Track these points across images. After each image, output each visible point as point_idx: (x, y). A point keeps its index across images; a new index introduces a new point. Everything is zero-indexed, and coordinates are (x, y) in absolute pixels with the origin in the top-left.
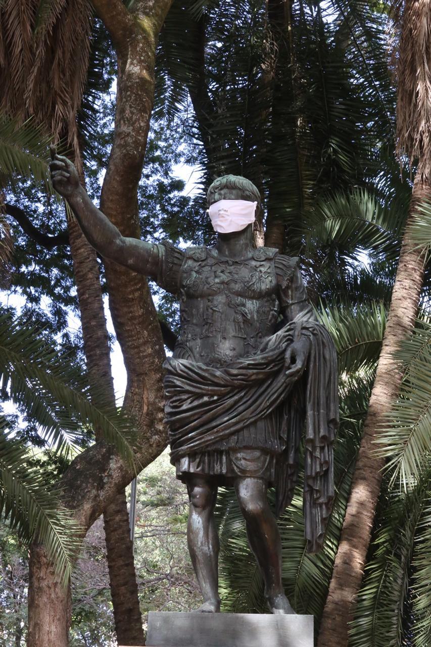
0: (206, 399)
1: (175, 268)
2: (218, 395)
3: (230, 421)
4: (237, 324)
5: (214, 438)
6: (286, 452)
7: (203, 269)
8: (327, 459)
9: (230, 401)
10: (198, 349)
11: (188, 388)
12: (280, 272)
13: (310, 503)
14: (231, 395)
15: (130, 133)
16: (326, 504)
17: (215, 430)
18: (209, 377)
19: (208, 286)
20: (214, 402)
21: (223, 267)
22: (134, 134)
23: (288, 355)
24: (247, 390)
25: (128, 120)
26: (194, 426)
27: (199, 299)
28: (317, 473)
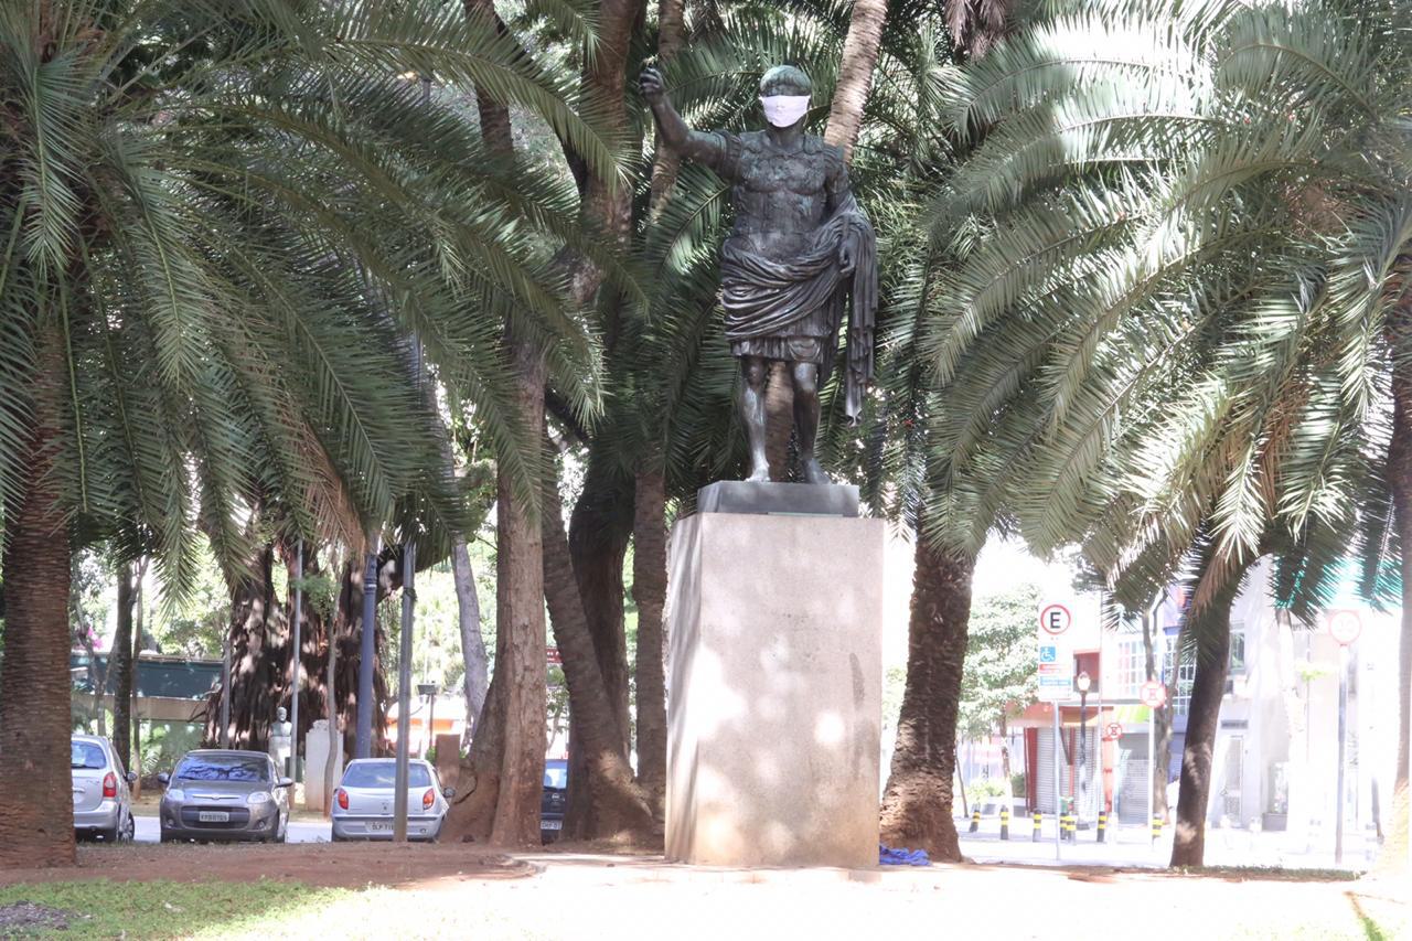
0: (769, 291)
9: (789, 295)
23: (842, 254)
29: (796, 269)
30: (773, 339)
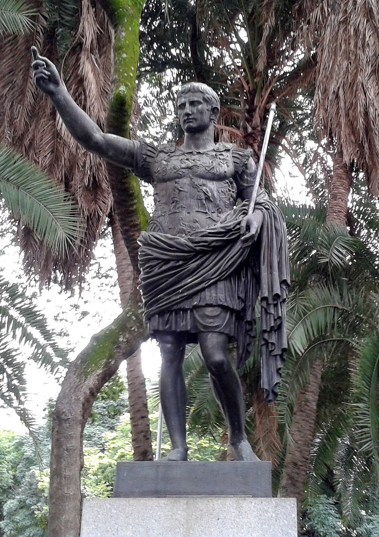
0: (171, 264)
1: (149, 159)
2: (183, 260)
3: (193, 282)
6: (244, 310)
7: (171, 158)
8: (280, 315)
9: (193, 266)
10: (166, 223)
11: (156, 255)
12: (237, 161)
13: (266, 355)
14: (194, 260)
16: (281, 356)
17: (181, 291)
18: (175, 244)
20: (180, 266)
21: (188, 156)
23: (244, 224)
24: (208, 256)
28: (272, 328)
29: (198, 239)
30: (177, 312)
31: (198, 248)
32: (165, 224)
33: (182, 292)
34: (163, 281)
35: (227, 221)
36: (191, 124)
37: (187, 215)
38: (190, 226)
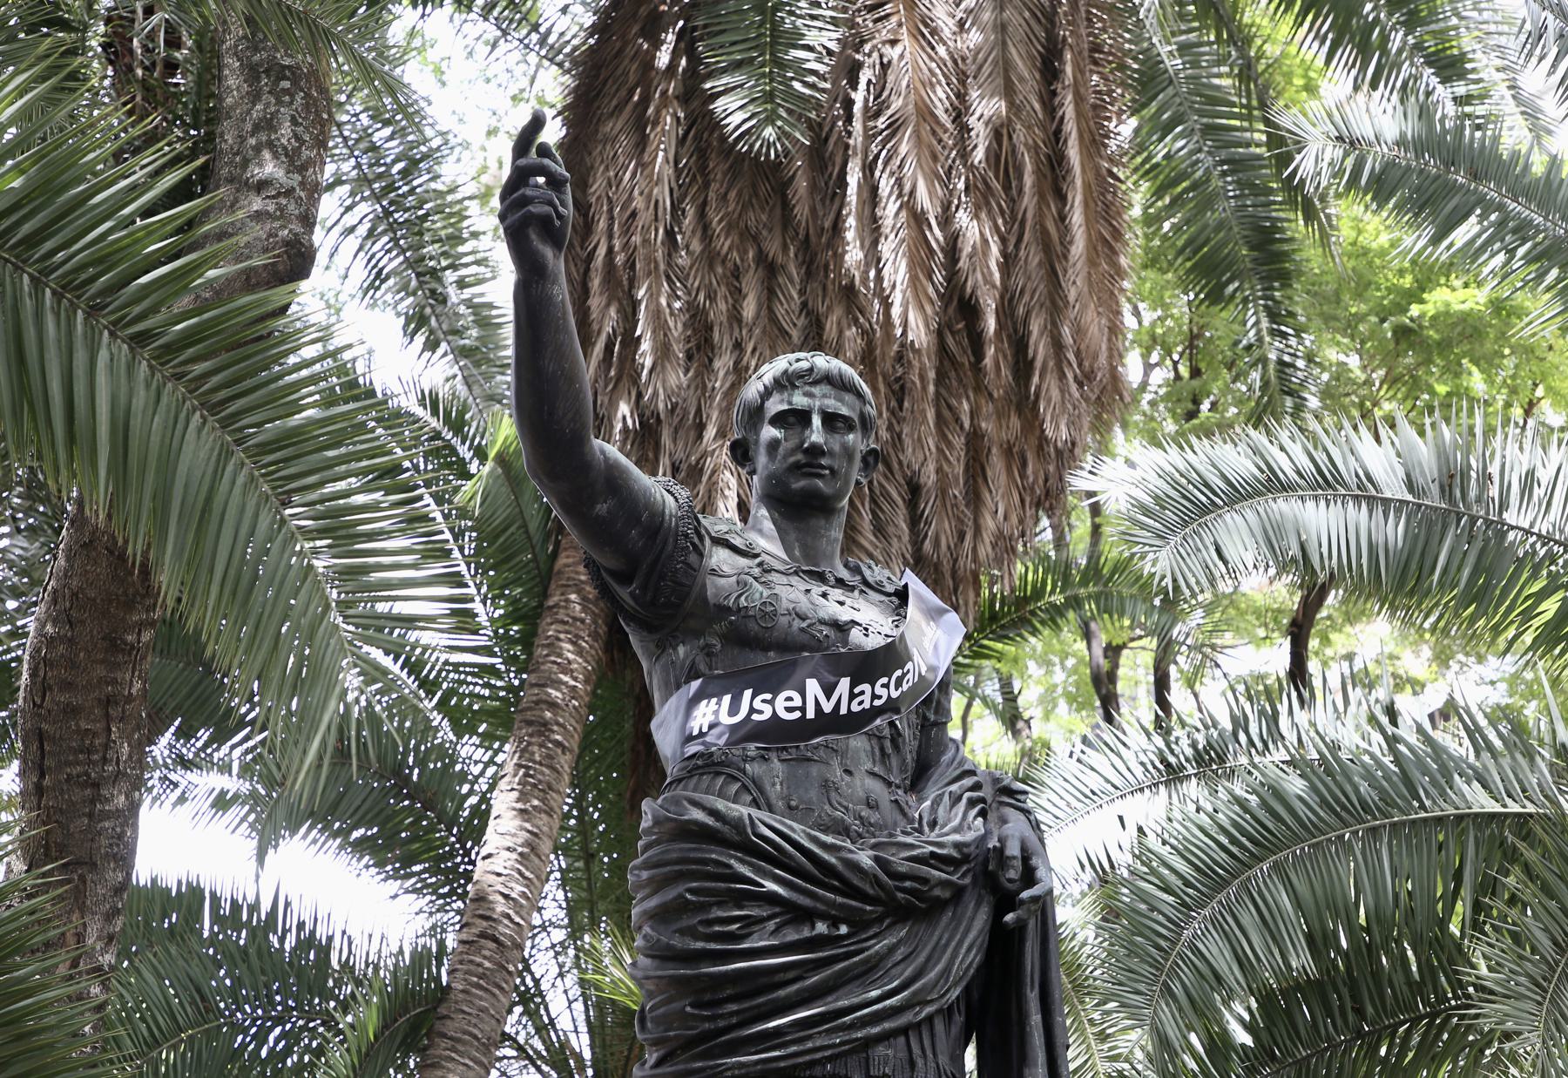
0: (821, 928)
2: (849, 925)
3: (888, 1002)
4: (874, 742)
5: (842, 1043)
11: (771, 886)
15: (293, 189)
18: (840, 867)
19: (804, 625)
22: (302, 194)
25: (286, 155)
26: (787, 997)
27: (772, 654)
29: (903, 868)
31: (900, 895)
32: (775, 791)
33: (852, 1026)
34: (791, 975)
35: (940, 821)
36: (820, 483)
37: (847, 778)
38: (861, 818)
